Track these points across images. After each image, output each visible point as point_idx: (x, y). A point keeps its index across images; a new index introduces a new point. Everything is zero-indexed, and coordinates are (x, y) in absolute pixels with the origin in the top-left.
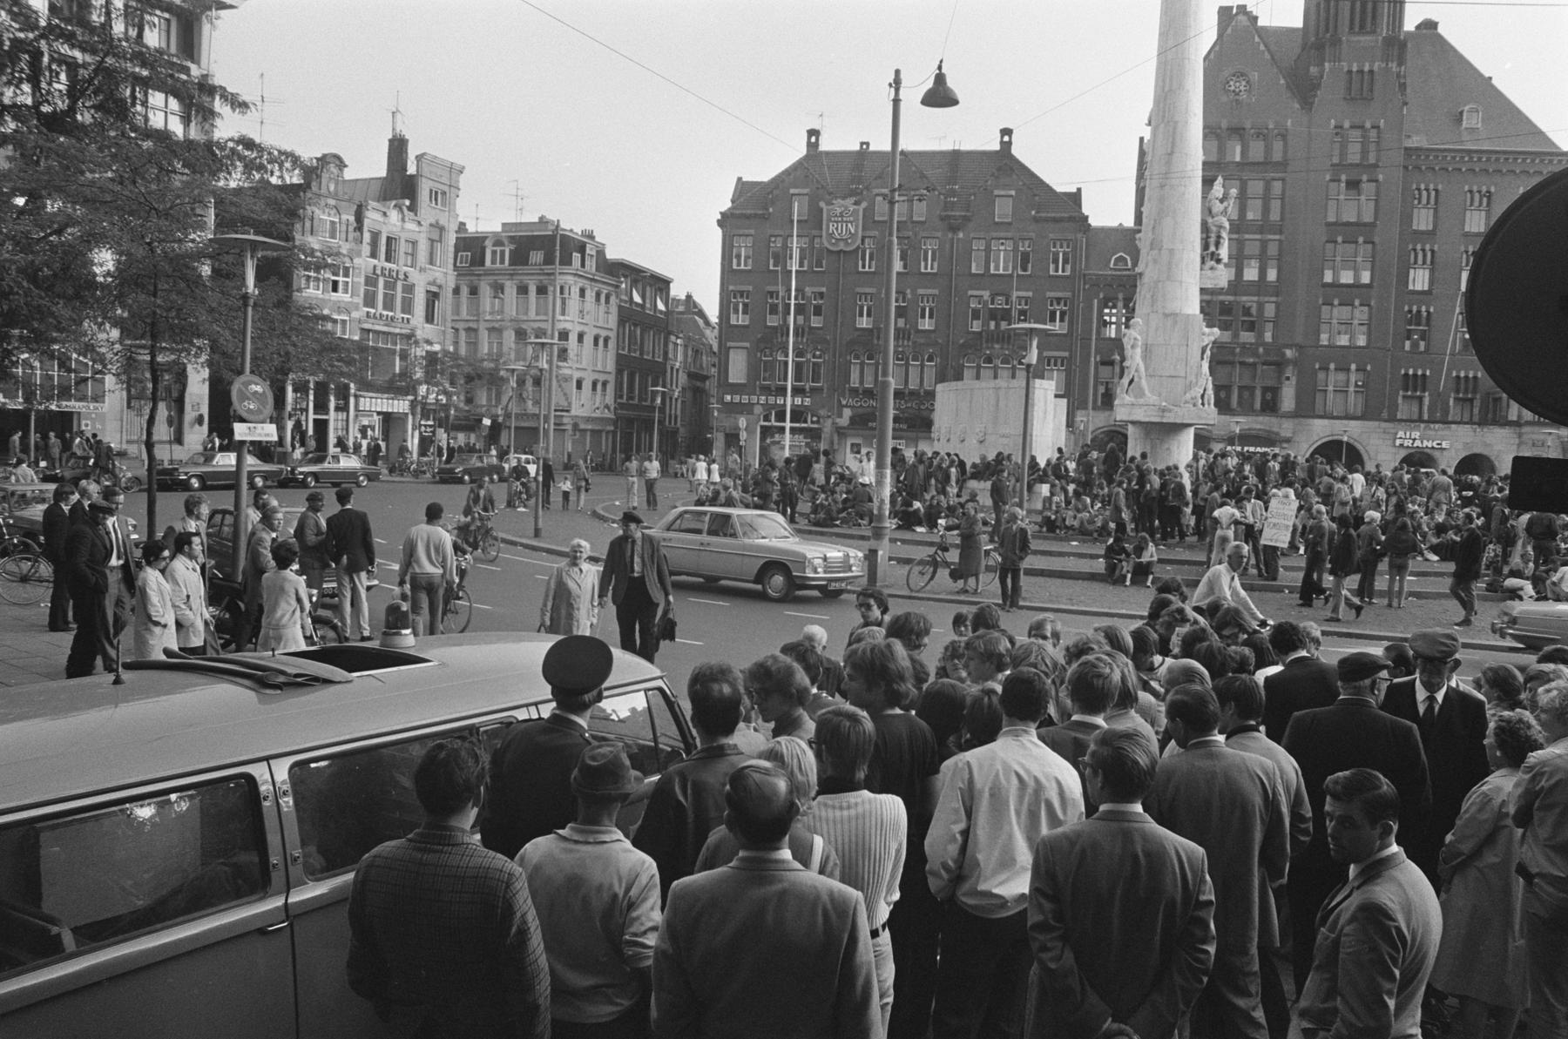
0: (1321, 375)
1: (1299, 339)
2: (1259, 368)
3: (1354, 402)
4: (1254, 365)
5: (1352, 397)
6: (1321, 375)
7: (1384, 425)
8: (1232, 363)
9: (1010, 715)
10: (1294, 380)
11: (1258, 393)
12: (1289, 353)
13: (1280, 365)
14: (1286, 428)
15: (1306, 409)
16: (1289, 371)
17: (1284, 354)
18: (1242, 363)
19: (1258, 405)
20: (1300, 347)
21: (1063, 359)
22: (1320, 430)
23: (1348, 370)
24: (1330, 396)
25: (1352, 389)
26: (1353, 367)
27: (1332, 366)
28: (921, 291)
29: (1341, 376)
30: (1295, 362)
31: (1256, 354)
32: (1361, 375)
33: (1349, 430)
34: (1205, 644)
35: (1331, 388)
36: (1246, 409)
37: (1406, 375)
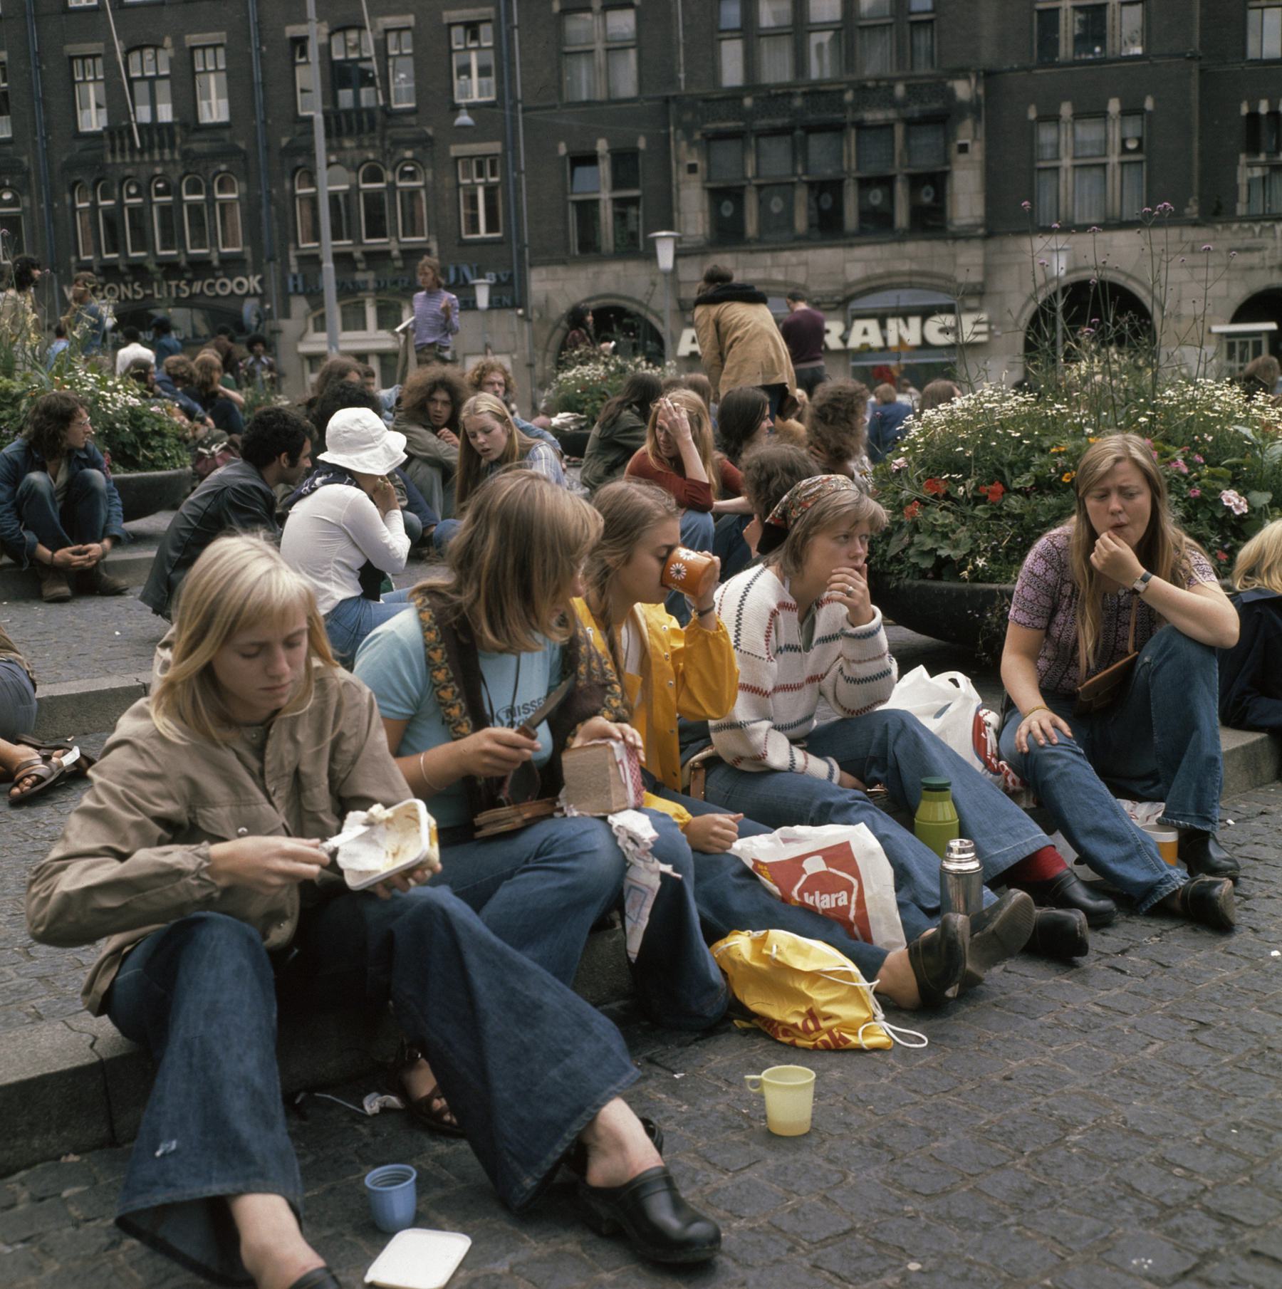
0: (1046, 135)
1: (988, 56)
2: (899, 130)
3: (1123, 190)
4: (888, 126)
5: (1114, 175)
6: (1046, 135)
7: (1191, 234)
8: (837, 128)
9: (432, 915)
10: (977, 151)
11: (901, 190)
12: (963, 90)
13: (942, 119)
14: (967, 262)
15: (1011, 214)
16: (966, 132)
17: (952, 93)
18: (860, 126)
19: (902, 217)
20: (989, 76)
21: (493, 158)
22: (1055, 259)
23: (1103, 115)
24: (1066, 177)
25: (1114, 159)
26: (1114, 106)
27: (1066, 110)
28: (192, 39)
29: (1089, 132)
30: (973, 108)
31: (892, 102)
32: (1134, 127)
33: (1121, 255)
34: (1166, 626)
35: (1066, 162)
36: (877, 224)
37: (1253, 116)
